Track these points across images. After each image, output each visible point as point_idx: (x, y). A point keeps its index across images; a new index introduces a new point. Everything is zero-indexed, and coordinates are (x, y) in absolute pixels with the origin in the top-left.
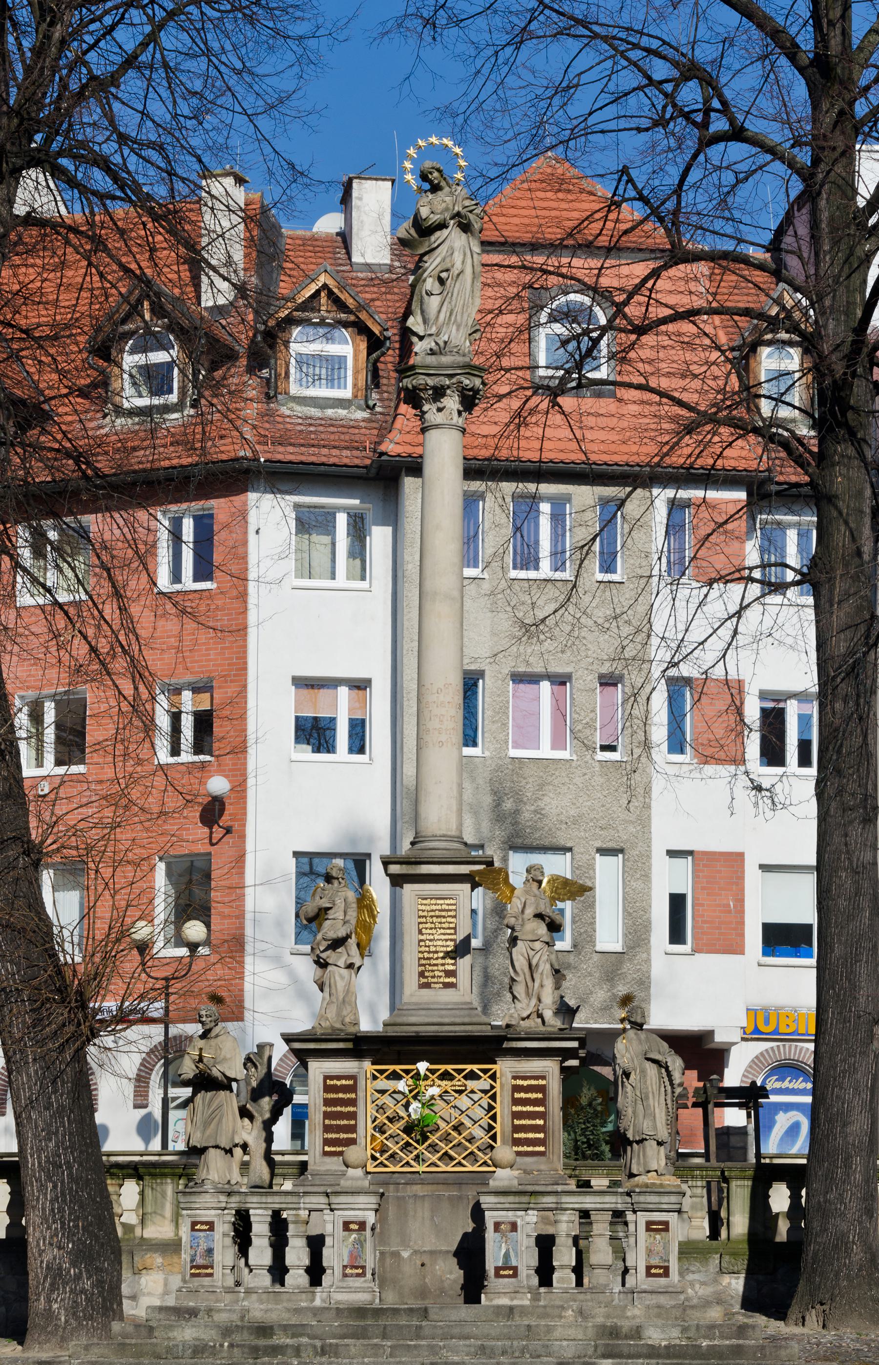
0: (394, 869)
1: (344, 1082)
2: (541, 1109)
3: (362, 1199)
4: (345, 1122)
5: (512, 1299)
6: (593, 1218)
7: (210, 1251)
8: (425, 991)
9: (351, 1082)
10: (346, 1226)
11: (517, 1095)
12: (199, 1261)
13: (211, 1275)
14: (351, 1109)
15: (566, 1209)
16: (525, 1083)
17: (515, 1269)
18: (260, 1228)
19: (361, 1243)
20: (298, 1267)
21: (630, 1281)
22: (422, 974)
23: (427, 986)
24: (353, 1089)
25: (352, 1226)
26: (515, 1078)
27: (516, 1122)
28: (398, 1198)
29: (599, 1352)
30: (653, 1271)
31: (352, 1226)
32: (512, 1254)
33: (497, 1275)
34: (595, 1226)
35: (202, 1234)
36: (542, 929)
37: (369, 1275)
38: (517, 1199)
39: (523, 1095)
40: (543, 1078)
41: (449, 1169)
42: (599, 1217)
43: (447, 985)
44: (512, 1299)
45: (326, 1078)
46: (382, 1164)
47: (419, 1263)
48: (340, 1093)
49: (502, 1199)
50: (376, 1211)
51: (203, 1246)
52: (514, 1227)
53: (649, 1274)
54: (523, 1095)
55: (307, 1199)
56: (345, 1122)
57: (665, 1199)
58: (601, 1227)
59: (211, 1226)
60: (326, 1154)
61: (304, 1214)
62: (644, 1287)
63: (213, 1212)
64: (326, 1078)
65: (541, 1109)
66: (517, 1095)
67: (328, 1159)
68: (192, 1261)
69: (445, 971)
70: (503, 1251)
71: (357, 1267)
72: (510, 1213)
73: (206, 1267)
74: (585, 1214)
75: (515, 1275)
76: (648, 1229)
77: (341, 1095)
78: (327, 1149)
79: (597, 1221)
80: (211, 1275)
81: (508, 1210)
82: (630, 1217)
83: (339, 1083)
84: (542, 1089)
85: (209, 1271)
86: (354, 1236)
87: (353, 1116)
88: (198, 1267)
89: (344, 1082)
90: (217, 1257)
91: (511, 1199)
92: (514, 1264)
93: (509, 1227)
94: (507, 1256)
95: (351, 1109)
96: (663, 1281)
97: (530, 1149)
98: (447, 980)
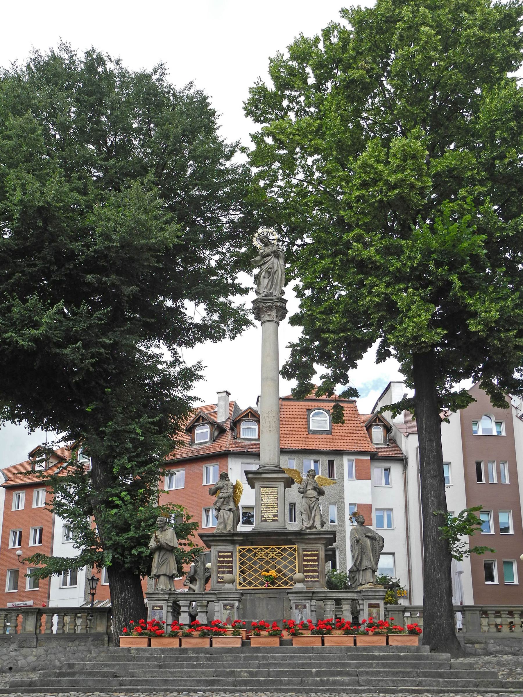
3: (232, 596)
6: (343, 603)
8: (263, 523)
15: (330, 599)
23: (266, 521)
24: (231, 556)
31: (228, 607)
36: (315, 494)
39: (308, 558)
40: (317, 551)
42: (345, 603)
43: (274, 520)
46: (244, 586)
50: (239, 601)
52: (305, 607)
54: (308, 558)
64: (219, 552)
74: (338, 602)
76: (369, 607)
81: (302, 600)
84: (317, 555)
86: (228, 611)
87: (231, 567)
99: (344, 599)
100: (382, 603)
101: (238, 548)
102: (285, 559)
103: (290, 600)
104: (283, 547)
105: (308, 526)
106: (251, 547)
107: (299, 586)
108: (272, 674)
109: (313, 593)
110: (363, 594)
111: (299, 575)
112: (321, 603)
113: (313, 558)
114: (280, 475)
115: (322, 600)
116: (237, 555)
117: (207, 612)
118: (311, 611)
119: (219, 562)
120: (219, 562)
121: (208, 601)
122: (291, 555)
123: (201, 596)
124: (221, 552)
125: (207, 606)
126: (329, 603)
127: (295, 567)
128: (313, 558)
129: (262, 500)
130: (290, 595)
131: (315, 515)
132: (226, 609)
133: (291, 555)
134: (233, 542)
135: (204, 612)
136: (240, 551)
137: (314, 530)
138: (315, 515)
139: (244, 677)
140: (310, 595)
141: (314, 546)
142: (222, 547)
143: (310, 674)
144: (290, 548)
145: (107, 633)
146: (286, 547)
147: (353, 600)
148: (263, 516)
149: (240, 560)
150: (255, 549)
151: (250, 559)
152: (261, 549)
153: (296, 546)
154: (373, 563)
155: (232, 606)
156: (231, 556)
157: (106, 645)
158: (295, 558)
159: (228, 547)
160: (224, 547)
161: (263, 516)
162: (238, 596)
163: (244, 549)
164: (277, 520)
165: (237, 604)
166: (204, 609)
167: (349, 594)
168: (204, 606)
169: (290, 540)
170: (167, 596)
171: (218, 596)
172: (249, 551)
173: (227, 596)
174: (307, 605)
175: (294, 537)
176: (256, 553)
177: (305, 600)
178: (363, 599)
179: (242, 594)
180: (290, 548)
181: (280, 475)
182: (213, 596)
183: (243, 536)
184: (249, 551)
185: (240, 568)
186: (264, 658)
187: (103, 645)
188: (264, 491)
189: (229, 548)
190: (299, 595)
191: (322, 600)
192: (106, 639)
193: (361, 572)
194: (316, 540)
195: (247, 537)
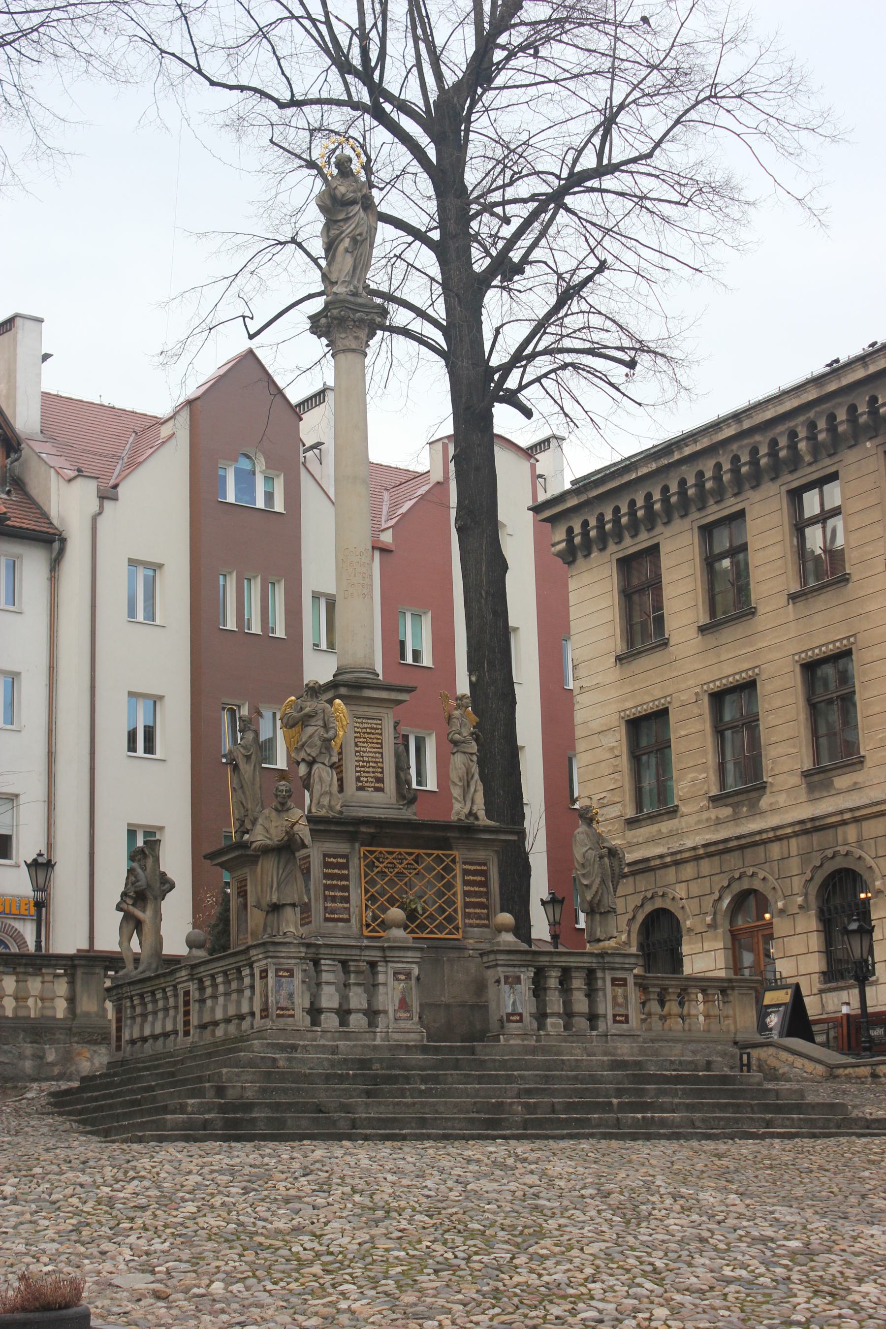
3: (409, 954)
6: (573, 974)
7: (291, 996)
11: (466, 878)
13: (293, 1016)
14: (345, 883)
16: (472, 868)
17: (520, 1015)
20: (358, 1011)
21: (602, 1026)
22: (358, 779)
24: (345, 866)
26: (465, 863)
27: (467, 899)
30: (618, 1018)
33: (509, 1021)
34: (574, 981)
38: (524, 957)
39: (471, 878)
40: (485, 864)
41: (424, 935)
43: (378, 789)
48: (335, 868)
52: (518, 980)
53: (615, 1021)
54: (471, 878)
58: (578, 983)
60: (327, 920)
62: (614, 1031)
63: (293, 961)
64: (325, 855)
66: (466, 878)
68: (277, 1003)
69: (374, 777)
72: (516, 969)
75: (521, 1021)
76: (613, 985)
77: (337, 871)
79: (576, 978)
80: (293, 1016)
81: (514, 966)
82: (599, 974)
88: (282, 1009)
90: (297, 1000)
91: (519, 957)
92: (520, 1011)
95: (345, 883)
96: (625, 1026)
110: (607, 959)
113: (479, 878)
123: (357, 952)
124: (330, 856)
126: (554, 974)
128: (479, 878)
132: (398, 980)
133: (448, 869)
134: (352, 837)
152: (400, 854)
153: (455, 853)
155: (408, 975)
156: (345, 866)
163: (371, 852)
164: (381, 790)
170: (303, 949)
171: (388, 953)
173: (401, 954)
177: (520, 966)
180: (448, 856)
189: (342, 847)
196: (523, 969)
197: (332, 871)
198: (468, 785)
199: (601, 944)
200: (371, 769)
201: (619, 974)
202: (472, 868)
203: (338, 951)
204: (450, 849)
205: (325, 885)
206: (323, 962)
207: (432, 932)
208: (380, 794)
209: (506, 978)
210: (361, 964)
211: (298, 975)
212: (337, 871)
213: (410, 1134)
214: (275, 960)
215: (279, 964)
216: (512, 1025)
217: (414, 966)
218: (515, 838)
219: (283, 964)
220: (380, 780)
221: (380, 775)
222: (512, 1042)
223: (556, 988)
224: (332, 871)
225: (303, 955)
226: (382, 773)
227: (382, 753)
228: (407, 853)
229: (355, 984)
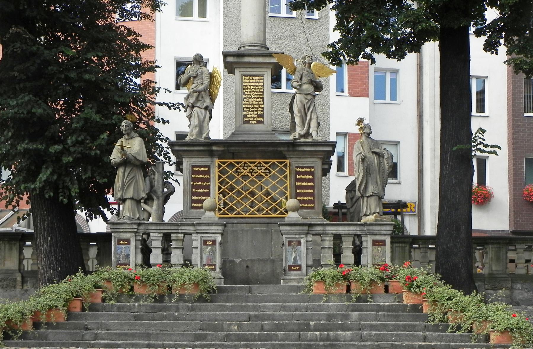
0: (230, 59)
1: (203, 169)
2: (312, 184)
3: (214, 228)
4: (204, 191)
5: (298, 283)
6: (343, 238)
7: (128, 256)
9: (207, 169)
10: (205, 242)
11: (298, 177)
12: (122, 261)
14: (207, 183)
15: (328, 234)
16: (303, 170)
18: (156, 243)
19: (214, 252)
23: (248, 122)
24: (208, 172)
25: (208, 243)
26: (297, 167)
27: (298, 191)
28: (233, 231)
29: (350, 309)
31: (208, 243)
32: (298, 258)
33: (290, 270)
34: (344, 243)
35: (123, 246)
37: (218, 269)
39: (302, 177)
40: (313, 167)
41: (261, 215)
42: (347, 238)
43: (259, 122)
44: (298, 283)
45: (193, 166)
47: (245, 266)
49: (293, 228)
50: (222, 234)
51: (124, 253)
52: (299, 243)
54: (302, 177)
55: (183, 228)
56: (204, 191)
57: (384, 228)
59: (129, 243)
60: (193, 207)
61: (181, 236)
63: (129, 235)
65: (312, 184)
66: (298, 177)
67: (194, 210)
68: (118, 261)
69: (257, 114)
70: (293, 256)
71: (211, 265)
72: (297, 236)
73: (126, 265)
74: (338, 237)
75: (300, 270)
77: (201, 176)
78: (193, 205)
79: (346, 240)
81: (296, 234)
83: (200, 169)
84: (312, 173)
85: (127, 267)
89: (203, 169)
90: (132, 259)
91: (298, 228)
92: (299, 263)
93: (296, 243)
94: (295, 259)
95: (207, 183)
97: (306, 205)
98: (259, 119)
99: (346, 234)
100: (388, 240)
101: (217, 161)
102: (274, 177)
103: (282, 234)
104: (272, 161)
105: (302, 133)
106: (232, 161)
107: (292, 216)
108: (265, 327)
109: (310, 225)
111: (292, 202)
112: (317, 238)
113: (308, 177)
114: (267, 60)
115: (319, 234)
116: (215, 172)
117: (183, 249)
118: (307, 249)
119: (194, 180)
120: (194, 180)
121: (185, 234)
122: (282, 172)
123: (176, 228)
125: (183, 241)
126: (328, 238)
127: (286, 188)
128: (308, 177)
129: (244, 94)
130: (282, 228)
131: (311, 119)
133: (282, 172)
134: (211, 154)
135: (180, 248)
136: (219, 166)
137: (309, 140)
138: (311, 119)
139: (235, 330)
140: (306, 228)
141: (309, 161)
142: (196, 160)
143: (308, 328)
144: (281, 163)
145: (20, 270)
146: (275, 161)
147: (356, 235)
148: (245, 116)
149: (220, 177)
150: (238, 163)
151: (231, 177)
153: (288, 161)
154: (380, 188)
155: (214, 242)
157: (19, 287)
158: (286, 177)
159: (204, 160)
160: (200, 160)
161: (245, 116)
162: (220, 228)
163: (224, 163)
164: (262, 122)
165: (219, 239)
166: (180, 244)
167: (352, 228)
168: (180, 240)
169: (281, 152)
172: (231, 165)
174: (303, 241)
175: (286, 149)
176: (238, 168)
177: (300, 234)
178: (366, 234)
179: (225, 226)
180: (281, 163)
181: (267, 60)
182: (191, 228)
183: (224, 146)
184: (231, 165)
185: (220, 188)
186: (255, 308)
187: (15, 287)
188: (247, 80)
190: (293, 228)
191: (319, 234)
192: (19, 279)
193: (365, 199)
194: (312, 154)
195: (228, 146)
196: (302, 236)
197: (198, 176)
198: (306, 116)
199: (368, 217)
200: (255, 109)
201: (379, 238)
202: (303, 170)
203: (161, 228)
204: (286, 159)
205: (193, 185)
206: (151, 234)
207: (267, 213)
208: (260, 125)
209: (290, 243)
210: (180, 235)
211: (133, 243)
212: (201, 176)
213: (123, 344)
214: (116, 234)
215: (119, 236)
216: (292, 272)
217: (216, 235)
218: (330, 149)
219: (123, 236)
220: (262, 116)
221: (262, 113)
222: (290, 284)
223: (329, 248)
224: (198, 176)
225: (136, 230)
226: (263, 111)
227: (263, 98)
228: (251, 163)
229: (175, 248)
